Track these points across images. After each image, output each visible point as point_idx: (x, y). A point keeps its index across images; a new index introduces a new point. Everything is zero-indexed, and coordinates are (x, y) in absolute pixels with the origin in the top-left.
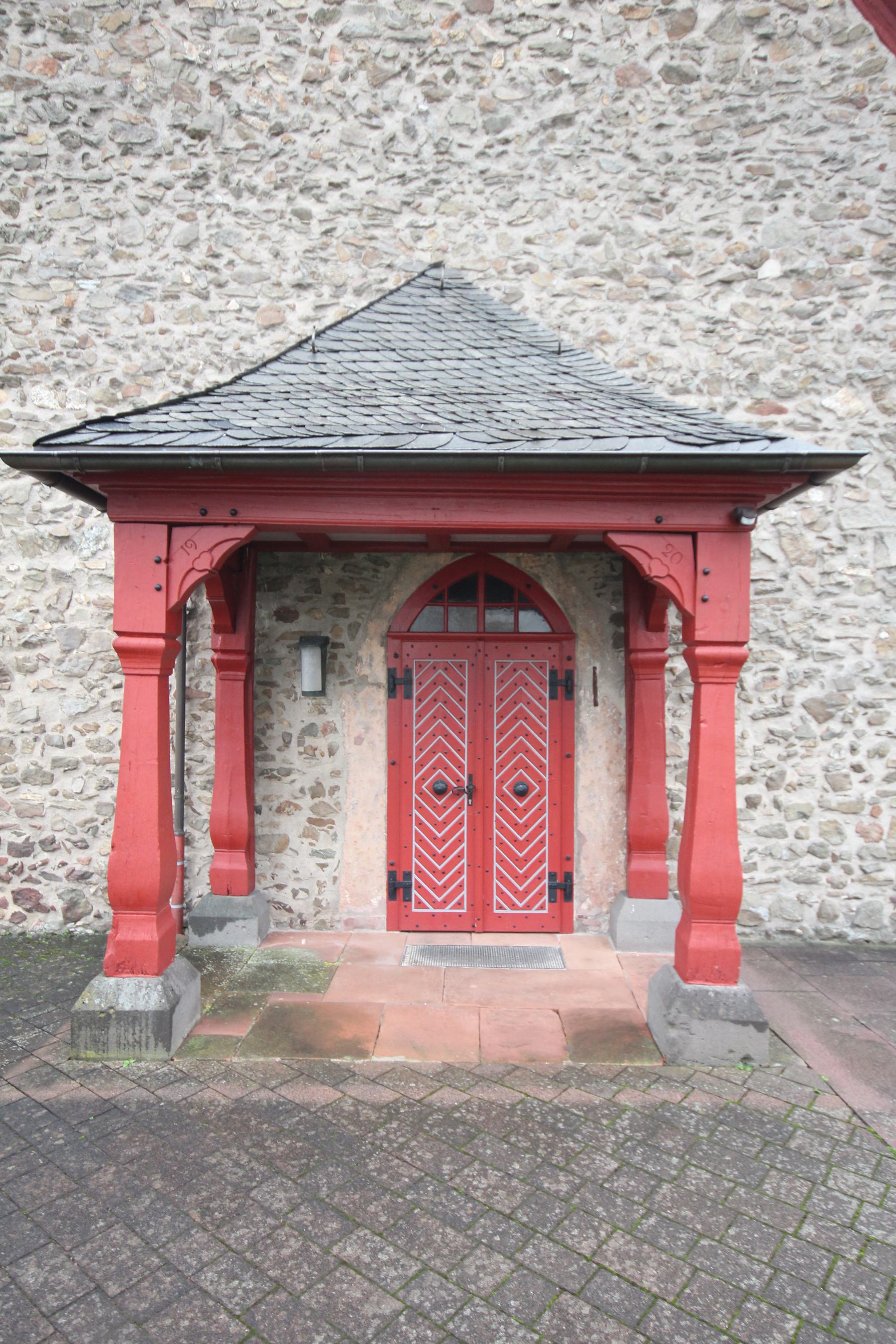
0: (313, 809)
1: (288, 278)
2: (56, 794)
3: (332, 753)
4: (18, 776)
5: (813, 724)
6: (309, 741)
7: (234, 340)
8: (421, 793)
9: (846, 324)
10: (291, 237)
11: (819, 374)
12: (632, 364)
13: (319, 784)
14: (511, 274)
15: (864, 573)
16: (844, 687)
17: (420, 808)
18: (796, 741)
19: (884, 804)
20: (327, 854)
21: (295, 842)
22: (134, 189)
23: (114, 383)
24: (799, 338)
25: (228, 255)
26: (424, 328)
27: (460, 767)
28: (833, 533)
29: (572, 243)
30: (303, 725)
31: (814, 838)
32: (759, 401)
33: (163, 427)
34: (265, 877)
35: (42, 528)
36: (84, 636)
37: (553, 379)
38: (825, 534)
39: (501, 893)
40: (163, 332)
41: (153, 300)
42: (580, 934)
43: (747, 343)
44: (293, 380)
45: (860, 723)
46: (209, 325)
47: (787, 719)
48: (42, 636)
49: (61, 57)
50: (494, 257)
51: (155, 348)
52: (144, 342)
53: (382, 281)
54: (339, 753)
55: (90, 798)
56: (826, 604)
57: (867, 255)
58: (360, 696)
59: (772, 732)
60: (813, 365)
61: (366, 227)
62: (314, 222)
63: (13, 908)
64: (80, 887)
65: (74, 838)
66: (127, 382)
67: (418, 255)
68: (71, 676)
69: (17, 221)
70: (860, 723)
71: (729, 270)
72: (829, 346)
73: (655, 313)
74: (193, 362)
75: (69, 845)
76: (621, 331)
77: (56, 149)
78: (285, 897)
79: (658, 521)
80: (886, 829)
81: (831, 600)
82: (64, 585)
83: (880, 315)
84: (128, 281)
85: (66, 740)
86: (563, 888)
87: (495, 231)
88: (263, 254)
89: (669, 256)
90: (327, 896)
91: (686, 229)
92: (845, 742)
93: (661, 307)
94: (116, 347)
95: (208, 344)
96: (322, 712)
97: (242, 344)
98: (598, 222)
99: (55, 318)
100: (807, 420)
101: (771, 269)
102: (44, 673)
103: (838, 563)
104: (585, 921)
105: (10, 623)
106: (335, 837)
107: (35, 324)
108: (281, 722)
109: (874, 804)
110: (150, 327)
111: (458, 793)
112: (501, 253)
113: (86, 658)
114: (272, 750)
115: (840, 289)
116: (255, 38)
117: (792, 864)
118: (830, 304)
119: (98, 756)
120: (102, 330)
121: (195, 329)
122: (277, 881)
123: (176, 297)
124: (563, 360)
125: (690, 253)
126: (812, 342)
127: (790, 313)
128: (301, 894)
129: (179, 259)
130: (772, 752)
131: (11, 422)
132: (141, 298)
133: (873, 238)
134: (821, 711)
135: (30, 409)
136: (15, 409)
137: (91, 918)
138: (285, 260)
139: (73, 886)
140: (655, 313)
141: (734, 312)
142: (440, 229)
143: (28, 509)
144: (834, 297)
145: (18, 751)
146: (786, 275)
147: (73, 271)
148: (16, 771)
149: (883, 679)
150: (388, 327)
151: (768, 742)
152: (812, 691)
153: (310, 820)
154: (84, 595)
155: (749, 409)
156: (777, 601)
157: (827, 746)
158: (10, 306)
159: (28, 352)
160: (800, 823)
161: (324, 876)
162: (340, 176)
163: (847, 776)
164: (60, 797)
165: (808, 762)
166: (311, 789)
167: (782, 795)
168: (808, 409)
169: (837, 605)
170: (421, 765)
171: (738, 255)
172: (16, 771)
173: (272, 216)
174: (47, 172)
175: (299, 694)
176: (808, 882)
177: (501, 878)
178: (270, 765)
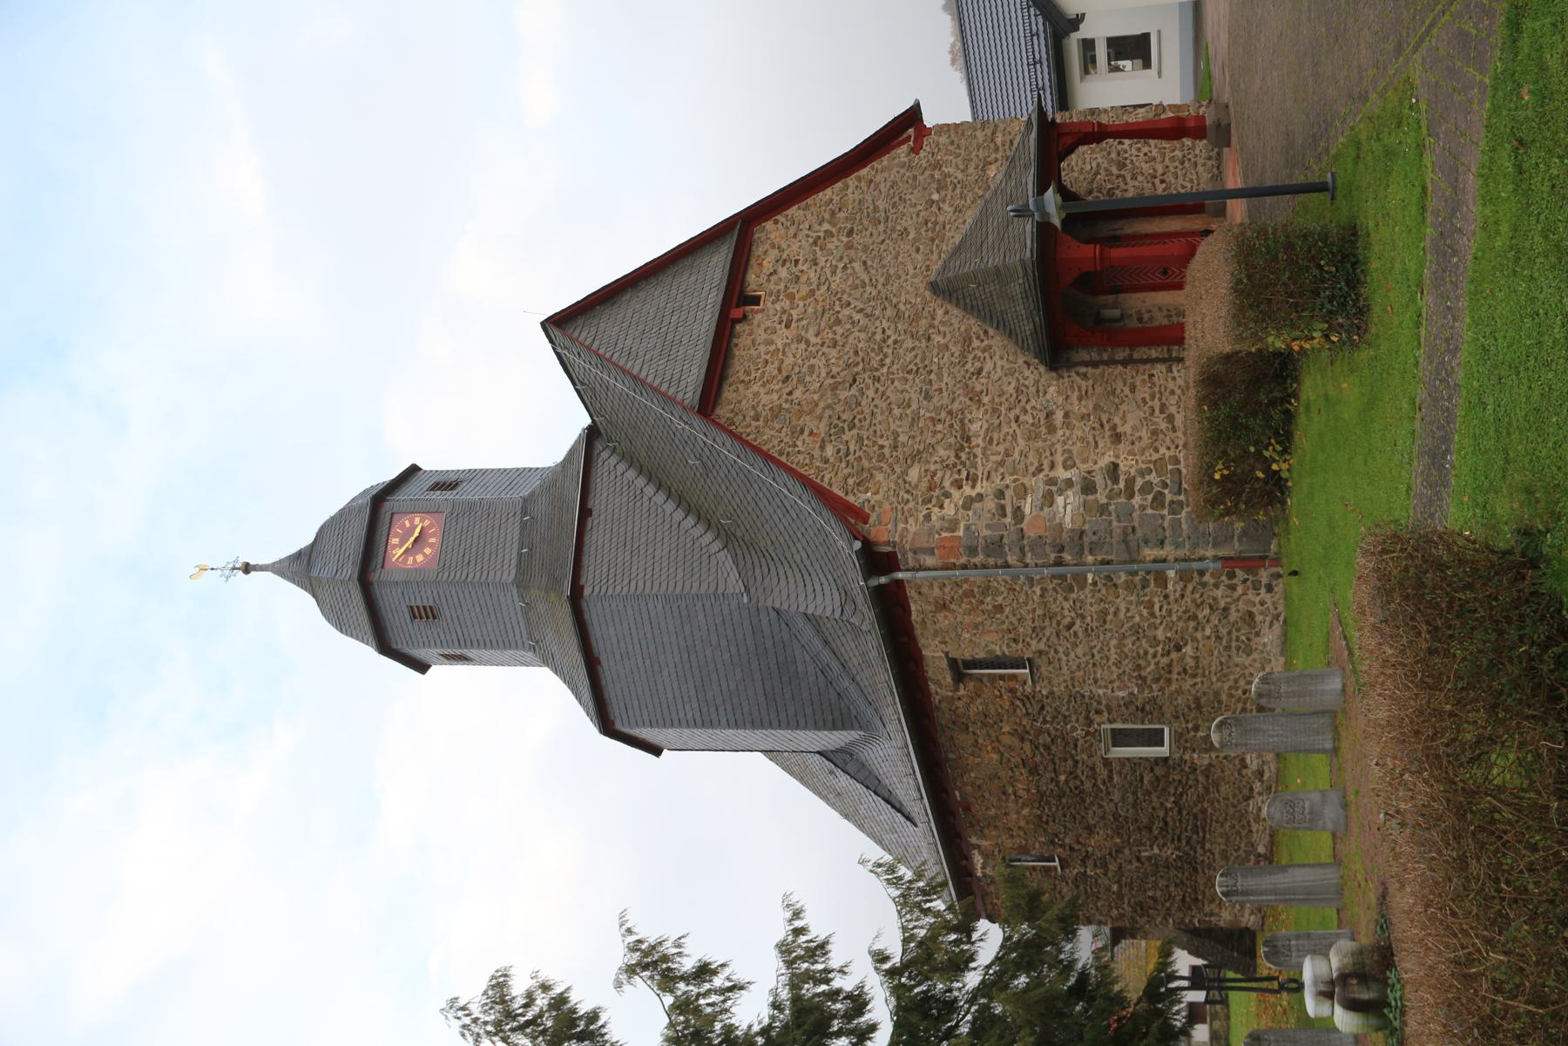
9: (960, 176)
22: (877, 402)
49: (811, 433)
77: (855, 432)
101: (936, 197)
102: (1117, 420)
116: (812, 367)
130: (1140, 178)
134: (1122, 166)
135: (982, 433)
152: (1115, 170)
162: (879, 330)
174: (865, 434)
176: (1196, 164)
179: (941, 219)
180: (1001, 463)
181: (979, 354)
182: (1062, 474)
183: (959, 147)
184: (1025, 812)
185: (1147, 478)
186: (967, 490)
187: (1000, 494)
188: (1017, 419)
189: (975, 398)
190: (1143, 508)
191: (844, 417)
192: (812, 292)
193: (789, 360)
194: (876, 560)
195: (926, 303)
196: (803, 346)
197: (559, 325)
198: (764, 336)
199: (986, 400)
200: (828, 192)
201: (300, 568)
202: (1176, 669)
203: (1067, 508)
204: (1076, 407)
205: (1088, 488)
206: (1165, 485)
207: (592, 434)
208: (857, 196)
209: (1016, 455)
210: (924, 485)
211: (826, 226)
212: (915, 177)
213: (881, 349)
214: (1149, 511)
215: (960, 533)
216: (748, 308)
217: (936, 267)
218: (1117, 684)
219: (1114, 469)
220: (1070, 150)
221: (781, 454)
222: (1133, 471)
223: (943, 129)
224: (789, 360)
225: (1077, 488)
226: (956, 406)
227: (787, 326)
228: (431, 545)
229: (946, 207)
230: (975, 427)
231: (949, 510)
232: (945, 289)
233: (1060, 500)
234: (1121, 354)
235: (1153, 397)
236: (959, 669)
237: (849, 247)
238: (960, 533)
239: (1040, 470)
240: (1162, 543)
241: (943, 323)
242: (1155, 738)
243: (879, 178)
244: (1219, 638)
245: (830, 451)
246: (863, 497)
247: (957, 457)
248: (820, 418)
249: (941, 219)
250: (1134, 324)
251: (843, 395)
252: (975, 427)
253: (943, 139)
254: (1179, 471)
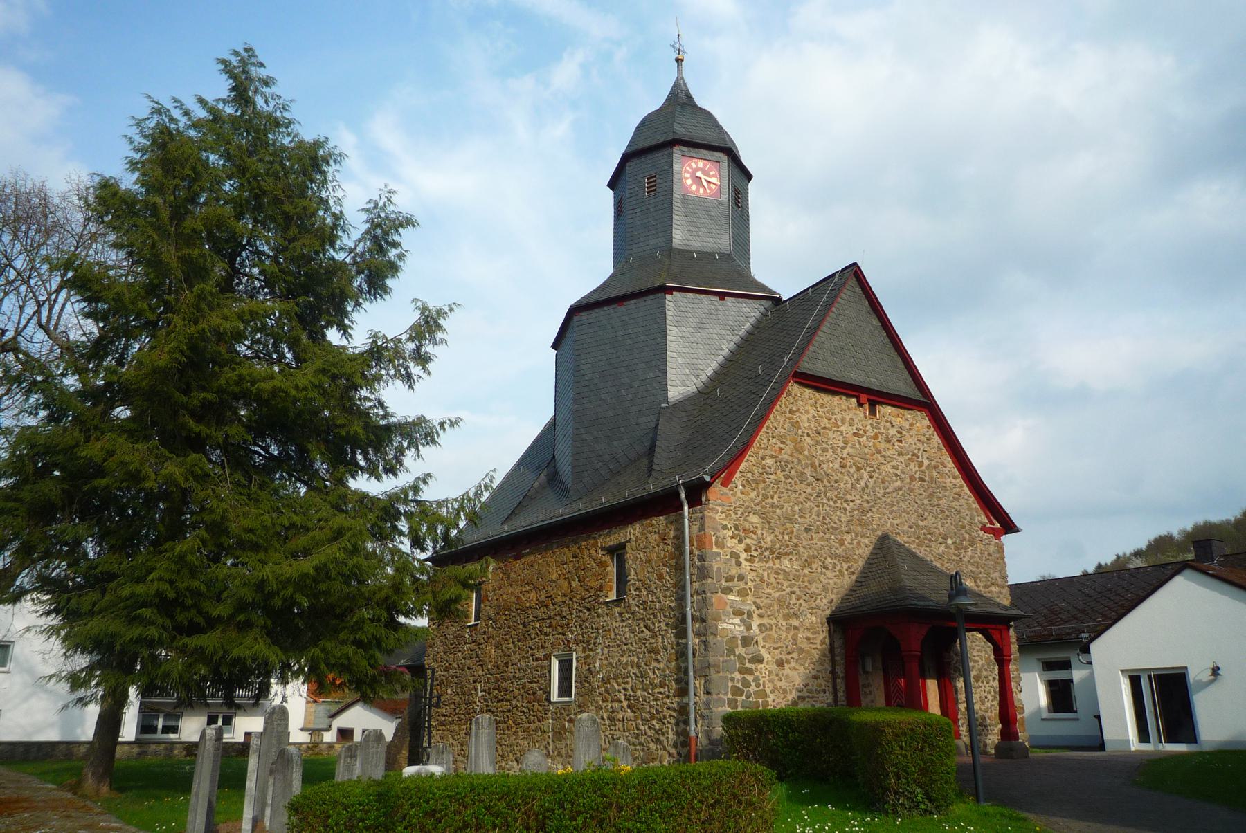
9: (966, 559)
16: (980, 670)
49: (781, 449)
101: (950, 541)
102: (793, 664)
116: (826, 450)
179: (933, 544)
180: (762, 580)
181: (838, 567)
184: (513, 599)
186: (743, 556)
187: (741, 578)
188: (792, 592)
189: (808, 563)
190: (733, 679)
191: (793, 472)
192: (879, 452)
193: (831, 435)
194: (697, 492)
195: (873, 530)
196: (841, 444)
197: (854, 272)
198: (848, 418)
199: (806, 571)
200: (951, 465)
201: (680, 99)
202: (616, 705)
203: (732, 626)
204: (802, 634)
205: (746, 641)
206: (748, 697)
207: (777, 301)
208: (949, 485)
210: (747, 525)
211: (926, 462)
212: (963, 527)
213: (839, 498)
214: (730, 684)
215: (715, 550)
216: (867, 406)
217: (898, 539)
218: (605, 662)
219: (758, 660)
220: (989, 638)
221: (768, 428)
222: (757, 674)
223: (1001, 549)
224: (831, 435)
226: (801, 549)
227: (854, 434)
228: (698, 190)
229: (942, 548)
230: (787, 563)
231: (730, 543)
232: (884, 546)
233: (737, 621)
234: (840, 670)
236: (617, 552)
237: (912, 478)
238: (715, 550)
240: (708, 693)
241: (859, 544)
242: (565, 690)
243: (963, 502)
244: (637, 736)
245: (769, 461)
246: (739, 483)
247: (767, 549)
248: (791, 455)
249: (933, 544)
250: (862, 681)
251: (808, 471)
253: (992, 548)
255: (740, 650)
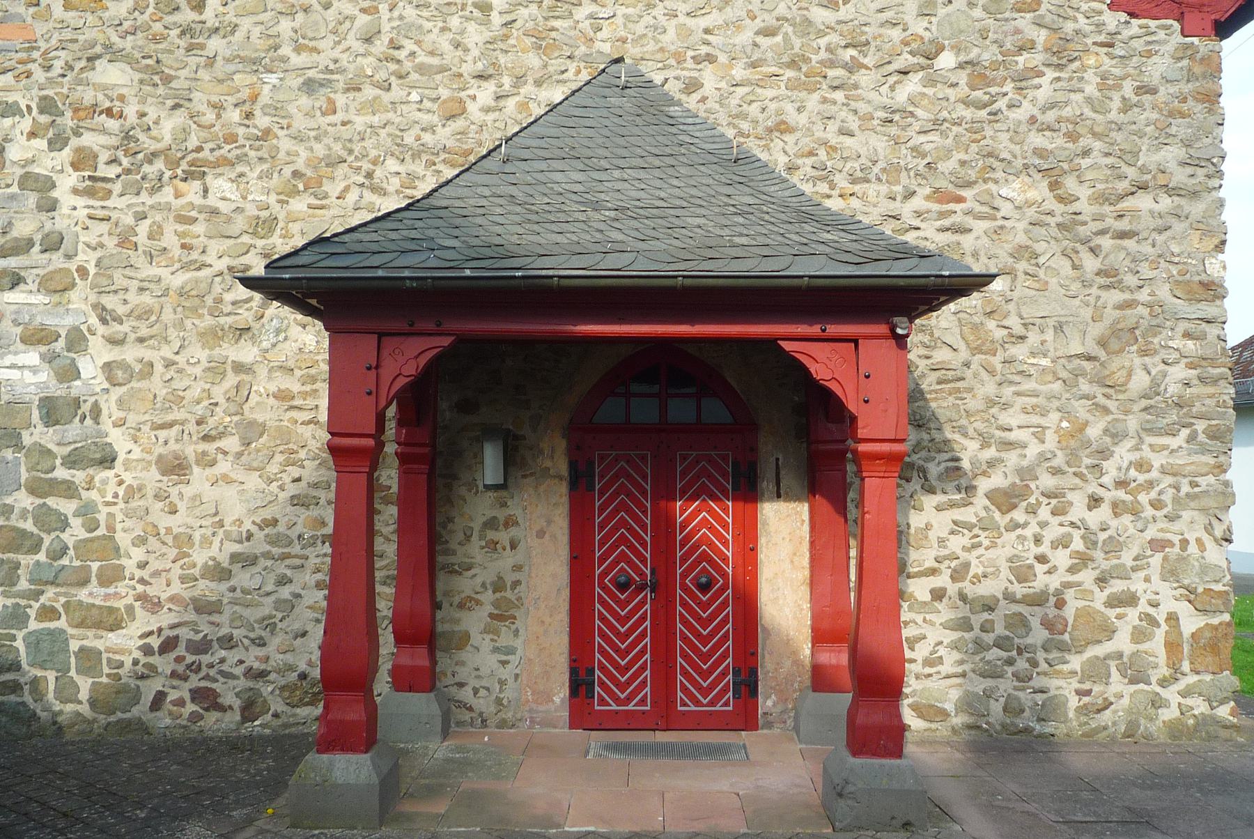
0: (496, 604)
1: (467, 69)
2: (233, 589)
3: (513, 546)
4: (196, 572)
5: (997, 515)
6: (491, 535)
7: (416, 130)
8: (604, 588)
10: (472, 27)
11: (996, 164)
12: (811, 154)
13: (500, 578)
14: (690, 64)
15: (1045, 362)
16: (1027, 474)
17: (603, 603)
18: (980, 532)
19: (1069, 595)
20: (511, 651)
21: (476, 638)
23: (296, 174)
24: (975, 129)
25: (409, 46)
26: (606, 132)
27: (644, 561)
28: (1014, 322)
29: (751, 34)
30: (485, 519)
31: (1000, 630)
32: (937, 190)
33: (375, 247)
34: (445, 675)
35: (222, 320)
36: (262, 429)
37: (729, 190)
38: (1005, 323)
39: (685, 690)
40: (344, 124)
41: (335, 92)
42: (765, 731)
43: (925, 132)
44: (487, 192)
45: (1044, 513)
46: (391, 115)
47: (970, 509)
48: (221, 429)
50: (672, 48)
51: (336, 139)
52: (326, 133)
53: (563, 72)
54: (521, 547)
55: (268, 594)
56: (1008, 391)
57: (1040, 47)
58: (542, 489)
59: (955, 522)
60: (990, 155)
61: (546, 19)
62: (494, 14)
63: (191, 707)
64: (259, 685)
65: (252, 635)
66: (309, 173)
67: (598, 45)
68: (250, 469)
69: (203, 17)
70: (1044, 513)
71: (905, 60)
72: (1004, 137)
73: (835, 103)
74: (373, 153)
75: (246, 642)
76: (802, 119)
78: (466, 695)
79: (824, 331)
80: (1071, 621)
81: (1013, 388)
82: (244, 377)
83: (1053, 105)
84: (311, 73)
85: (244, 535)
86: (747, 685)
87: (674, 22)
88: (445, 44)
89: (846, 47)
90: (508, 694)
91: (863, 19)
92: (1029, 532)
93: (839, 96)
94: (298, 138)
95: (389, 135)
96: (504, 505)
97: (422, 134)
98: (775, 13)
99: (238, 111)
100: (985, 209)
101: (946, 60)
102: (224, 466)
103: (1019, 351)
104: (770, 718)
105: (189, 416)
106: (516, 633)
107: (219, 116)
108: (462, 515)
109: (1058, 593)
110: (331, 119)
111: (641, 588)
112: (680, 44)
113: (266, 451)
114: (453, 545)
115: (1013, 80)
117: (977, 658)
118: (1005, 94)
119: (276, 551)
120: (284, 122)
121: (375, 120)
122: (457, 679)
123: (360, 89)
124: (739, 169)
125: (867, 43)
126: (989, 132)
127: (966, 102)
128: (482, 692)
129: (362, 51)
130: (957, 544)
131: (194, 214)
132: (323, 91)
133: (1044, 32)
134: (1006, 500)
135: (212, 201)
136: (198, 201)
137: (268, 717)
138: (466, 50)
139: (251, 684)
140: (835, 103)
141: (911, 101)
142: (619, 20)
143: (209, 301)
144: (1009, 87)
145: (197, 546)
146: (961, 66)
147: (255, 64)
148: (194, 566)
149: (1066, 468)
150: (573, 132)
151: (952, 533)
152: (997, 480)
153: (491, 616)
154: (263, 385)
155: (928, 198)
156: (958, 390)
157: (1013, 535)
158: (195, 100)
159: (211, 145)
160: (986, 616)
161: (505, 673)
163: (1031, 567)
164: (238, 594)
165: (991, 554)
166: (492, 583)
167: (966, 586)
168: (986, 198)
169: (1018, 394)
170: (602, 560)
171: (914, 46)
172: (194, 566)
173: (454, 9)
175: (481, 488)
176: (996, 675)
177: (685, 673)
178: (452, 559)
182: (89, 368)
183: (1126, 107)
185: (76, 522)
187: (53, 243)
199: (299, 205)
205: (53, 411)
209: (153, 271)
222: (94, 495)
225: (56, 390)
233: (32, 357)
235: (273, 540)
239: (105, 316)
249: (865, 79)
252: (221, 185)
254: (84, 582)
255: (37, 434)
